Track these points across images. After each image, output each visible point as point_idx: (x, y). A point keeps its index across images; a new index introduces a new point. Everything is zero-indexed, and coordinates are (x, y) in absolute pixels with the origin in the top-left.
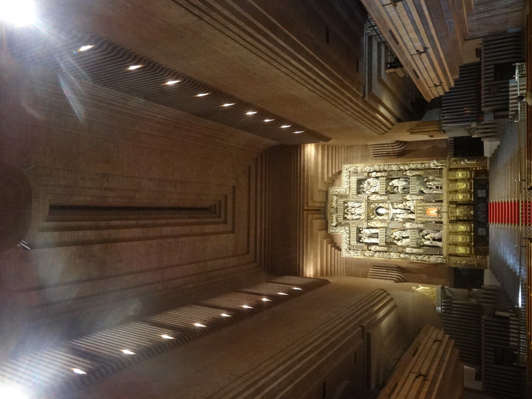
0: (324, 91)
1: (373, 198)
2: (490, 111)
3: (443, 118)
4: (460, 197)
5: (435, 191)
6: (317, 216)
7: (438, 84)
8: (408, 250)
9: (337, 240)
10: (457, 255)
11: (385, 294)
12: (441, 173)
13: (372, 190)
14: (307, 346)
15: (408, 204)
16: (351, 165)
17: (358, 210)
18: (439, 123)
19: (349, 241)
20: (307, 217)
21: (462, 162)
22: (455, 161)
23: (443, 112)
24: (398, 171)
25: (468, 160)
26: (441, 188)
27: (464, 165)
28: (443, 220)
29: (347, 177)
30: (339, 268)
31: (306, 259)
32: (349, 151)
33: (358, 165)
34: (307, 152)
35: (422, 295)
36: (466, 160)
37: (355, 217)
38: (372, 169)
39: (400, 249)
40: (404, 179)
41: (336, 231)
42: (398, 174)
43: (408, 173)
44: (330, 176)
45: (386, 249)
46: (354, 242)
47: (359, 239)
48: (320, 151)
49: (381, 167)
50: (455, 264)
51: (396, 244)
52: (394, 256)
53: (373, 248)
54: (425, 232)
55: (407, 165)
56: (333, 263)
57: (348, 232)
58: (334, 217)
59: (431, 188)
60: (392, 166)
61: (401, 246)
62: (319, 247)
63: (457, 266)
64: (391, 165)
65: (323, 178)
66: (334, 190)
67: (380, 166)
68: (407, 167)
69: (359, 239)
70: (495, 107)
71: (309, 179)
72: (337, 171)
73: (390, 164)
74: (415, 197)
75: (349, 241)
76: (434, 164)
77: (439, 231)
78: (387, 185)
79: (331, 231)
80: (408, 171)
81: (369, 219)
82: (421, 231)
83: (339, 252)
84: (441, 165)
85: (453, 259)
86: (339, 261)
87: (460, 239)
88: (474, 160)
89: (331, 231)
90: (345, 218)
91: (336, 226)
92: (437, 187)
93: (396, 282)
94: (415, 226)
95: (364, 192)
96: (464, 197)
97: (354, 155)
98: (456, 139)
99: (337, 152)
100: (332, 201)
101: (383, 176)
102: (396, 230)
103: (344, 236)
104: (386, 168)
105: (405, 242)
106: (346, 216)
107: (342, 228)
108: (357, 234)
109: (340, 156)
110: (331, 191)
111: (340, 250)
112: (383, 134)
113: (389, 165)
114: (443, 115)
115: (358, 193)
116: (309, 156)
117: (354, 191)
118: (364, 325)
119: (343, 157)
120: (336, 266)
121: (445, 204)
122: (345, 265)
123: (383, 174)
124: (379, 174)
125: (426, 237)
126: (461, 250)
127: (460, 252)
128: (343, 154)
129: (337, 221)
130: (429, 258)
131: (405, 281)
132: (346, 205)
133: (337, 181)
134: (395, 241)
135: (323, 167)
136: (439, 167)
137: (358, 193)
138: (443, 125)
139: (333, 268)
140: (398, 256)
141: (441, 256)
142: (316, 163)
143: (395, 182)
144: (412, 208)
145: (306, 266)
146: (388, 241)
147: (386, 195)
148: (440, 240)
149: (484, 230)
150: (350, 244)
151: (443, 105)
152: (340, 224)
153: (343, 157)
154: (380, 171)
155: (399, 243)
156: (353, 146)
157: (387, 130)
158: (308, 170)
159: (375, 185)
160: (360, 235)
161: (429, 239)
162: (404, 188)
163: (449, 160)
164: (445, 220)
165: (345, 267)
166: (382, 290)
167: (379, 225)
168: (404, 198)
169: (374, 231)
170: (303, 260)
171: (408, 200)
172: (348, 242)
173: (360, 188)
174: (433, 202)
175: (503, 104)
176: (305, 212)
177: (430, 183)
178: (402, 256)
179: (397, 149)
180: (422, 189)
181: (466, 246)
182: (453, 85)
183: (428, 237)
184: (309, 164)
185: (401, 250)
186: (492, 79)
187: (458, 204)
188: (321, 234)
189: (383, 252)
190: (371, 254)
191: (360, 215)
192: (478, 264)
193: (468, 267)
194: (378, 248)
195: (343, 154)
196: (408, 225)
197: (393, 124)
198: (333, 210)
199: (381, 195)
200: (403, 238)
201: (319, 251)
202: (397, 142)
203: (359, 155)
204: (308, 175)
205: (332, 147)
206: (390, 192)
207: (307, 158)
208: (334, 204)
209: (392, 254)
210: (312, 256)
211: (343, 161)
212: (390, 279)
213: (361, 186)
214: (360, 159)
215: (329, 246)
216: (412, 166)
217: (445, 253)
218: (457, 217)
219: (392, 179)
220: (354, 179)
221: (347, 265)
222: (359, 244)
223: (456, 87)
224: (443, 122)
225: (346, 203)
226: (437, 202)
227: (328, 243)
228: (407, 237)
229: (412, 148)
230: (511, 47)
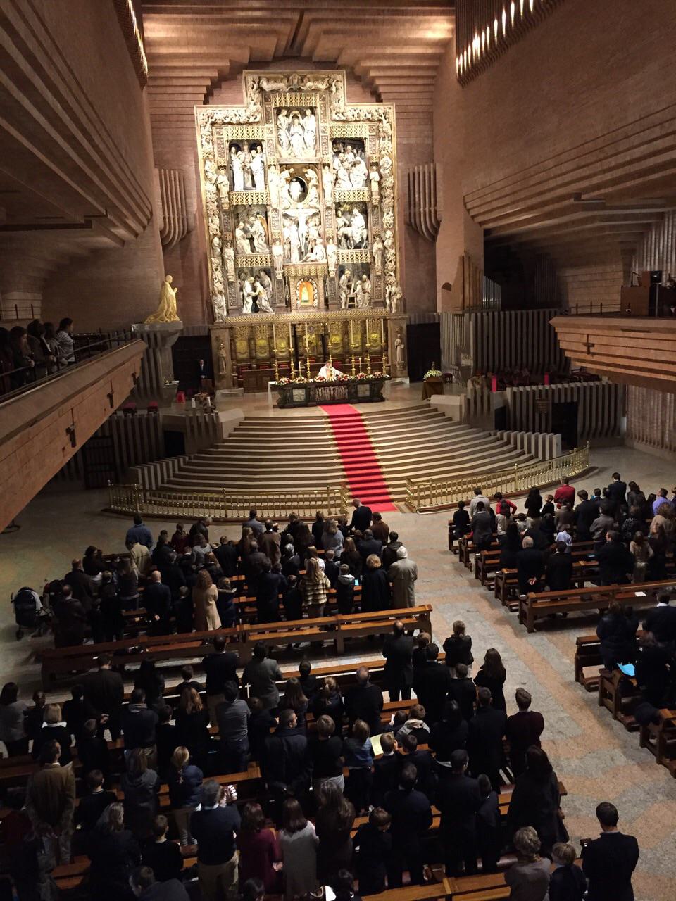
0: (635, 140)
2: (505, 401)
3: (485, 314)
4: (336, 339)
5: (344, 295)
6: (283, 43)
7: (592, 350)
8: (229, 252)
9: (225, 92)
10: (232, 340)
11: (145, 222)
12: (376, 304)
13: (342, 173)
14: (90, 140)
15: (319, 249)
16: (394, 124)
18: (477, 307)
19: (230, 123)
20: (285, 21)
21: (398, 340)
22: (401, 328)
23: (496, 314)
24: (382, 226)
25: (403, 350)
26: (350, 306)
27: (393, 343)
28: (294, 312)
29: (369, 116)
30: (165, 97)
31: (185, 21)
32: (421, 115)
33: (394, 139)
34: (435, 21)
35: (161, 296)
36: (402, 346)
37: (283, 132)
38: (388, 171)
39: (229, 234)
40: (365, 236)
41: (251, 92)
42: (375, 225)
43: (377, 246)
44: (372, 74)
45: (226, 207)
46: (228, 134)
47: (236, 145)
48: (430, 51)
49: (389, 192)
50: (218, 339)
51: (237, 225)
52: (214, 224)
53: (223, 179)
54: (267, 280)
55: (394, 243)
56: (175, 82)
57: (251, 120)
58: (281, 85)
59: (349, 287)
60: (391, 214)
61: (234, 237)
62: (213, 50)
63: (214, 344)
64: (393, 211)
65: (370, 57)
66: (340, 85)
67: (392, 188)
68: (388, 243)
69: (236, 145)
70: (511, 408)
71: (372, 27)
72: (381, 89)
73: (396, 210)
74: (332, 261)
75: (230, 123)
76: (395, 294)
77: (272, 305)
78: (351, 203)
79: (250, 79)
80: (380, 246)
82: (269, 272)
83: (202, 97)
84: (393, 305)
85: (226, 335)
86: (180, 97)
87: (261, 342)
88: (403, 359)
89: (250, 77)
90: (279, 111)
91: (261, 90)
92: (352, 300)
93: (162, 232)
94: (278, 264)
95: (337, 153)
96: (337, 344)
97: (413, 128)
98: (437, 326)
99: (421, 88)
100: (316, 79)
101: (371, 195)
102: (265, 226)
103: (241, 111)
104: (387, 201)
105: (245, 244)
106: (284, 112)
107: (258, 106)
108: (248, 140)
109: (414, 96)
110: (339, 77)
111: (206, 102)
112: (465, 204)
113: (393, 207)
114: (490, 314)
115: (335, 141)
116: (426, 26)
118: (109, 216)
119: (409, 102)
120: (169, 90)
121: (322, 314)
122: (174, 111)
123: (376, 197)
124: (375, 187)
125: (258, 284)
126: (242, 346)
127: (238, 344)
128: (418, 102)
129: (272, 91)
130: (220, 293)
131: (164, 248)
132: (308, 112)
133: (357, 89)
134: (241, 224)
135: (393, 57)
136: (388, 301)
137: (335, 141)
138: (473, 315)
139: (163, 83)
140: (215, 232)
141: (225, 313)
142: (407, 42)
143: (358, 220)
144: (312, 256)
145: (168, 20)
146: (240, 210)
148: (256, 309)
149: (303, 398)
151: (507, 313)
152: (267, 100)
153: (409, 102)
154: (381, 188)
155: (239, 233)
156: (432, 124)
157: (472, 213)
158: (394, 21)
159: (353, 180)
160: (246, 148)
161: (254, 290)
162: (347, 237)
163: (403, 319)
164: (295, 315)
165: (170, 111)
166: (151, 213)
168: (331, 241)
169: (259, 179)
170: (182, 12)
171: (325, 248)
172: (228, 120)
173: (345, 146)
174: (325, 293)
175: (515, 422)
176: (296, 16)
177: (359, 287)
178: (216, 241)
179: (424, 224)
180: (348, 272)
181: (250, 353)
182: (567, 354)
183: (260, 288)
184: (408, 25)
185: (227, 239)
186: (556, 401)
187: (323, 338)
188: (244, 56)
189: (218, 200)
190: (209, 175)
192: (223, 377)
193: (215, 359)
194: (225, 190)
195: (418, 102)
197: (481, 224)
198: (296, 81)
200: (251, 239)
201: (204, 50)
202: (438, 223)
203: (413, 141)
204: (383, 22)
205: (433, 77)
207: (421, 22)
208: (309, 84)
209: (217, 220)
210: (192, 35)
211: (401, 103)
212: (164, 218)
213: (349, 147)
214: (405, 142)
215: (215, 74)
216: (390, 253)
217: (234, 319)
218: (301, 337)
219: (364, 212)
220: (364, 131)
221: (175, 118)
222: (226, 145)
223: (564, 360)
224: (479, 314)
225: (313, 113)
226: (326, 301)
227: (220, 70)
228: (253, 249)
230: (600, 423)
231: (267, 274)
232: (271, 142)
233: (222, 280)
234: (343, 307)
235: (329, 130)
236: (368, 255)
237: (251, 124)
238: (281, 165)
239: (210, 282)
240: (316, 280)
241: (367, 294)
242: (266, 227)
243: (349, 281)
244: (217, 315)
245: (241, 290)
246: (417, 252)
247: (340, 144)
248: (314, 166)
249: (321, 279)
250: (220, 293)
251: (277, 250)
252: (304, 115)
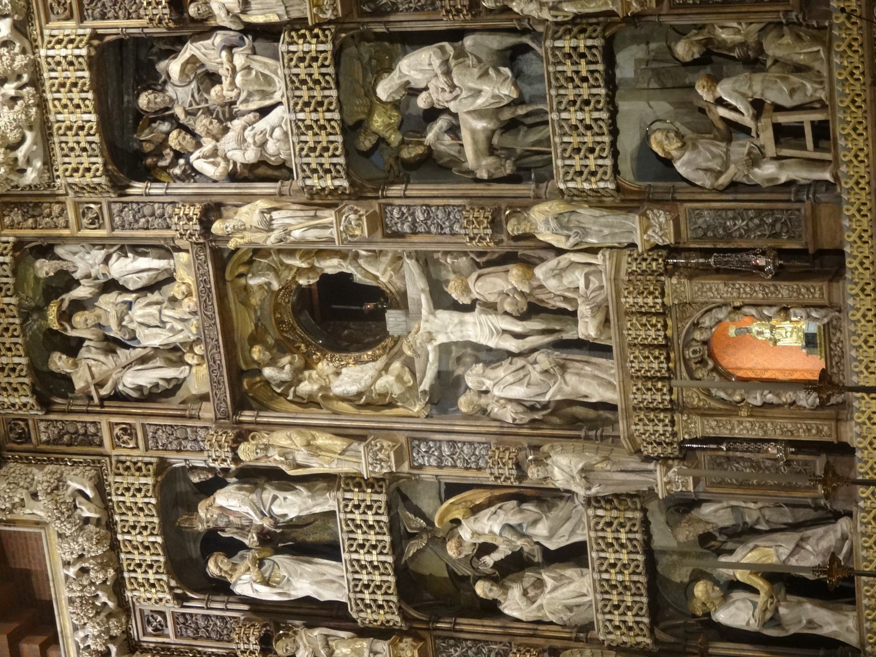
1: (247, 221)
15: (552, 280)
17: (149, 320)
19: (118, 588)
40: (496, 42)
51: (491, 609)
74: (600, 226)
81: (245, 394)
90: (51, 388)
106: (59, 362)
117: (82, 162)
132: (44, 268)
134: (482, 589)
147: (357, 194)
150: (125, 608)
152: (25, 437)
167: (331, 456)
169: (292, 505)
174: (753, 273)
191: (174, 354)
196: (563, 467)
199: (317, 201)
206: (382, 161)
213: (144, 100)
222: (197, 607)
225: (46, 250)
232: (162, 438)
234: (827, 176)
235: (86, 197)
236: (566, 44)
237: (107, 507)
238: (240, 402)
241: (774, 49)
242: (480, 497)
247: (130, 155)
248: (224, 265)
251: (563, 467)
252: (66, 281)
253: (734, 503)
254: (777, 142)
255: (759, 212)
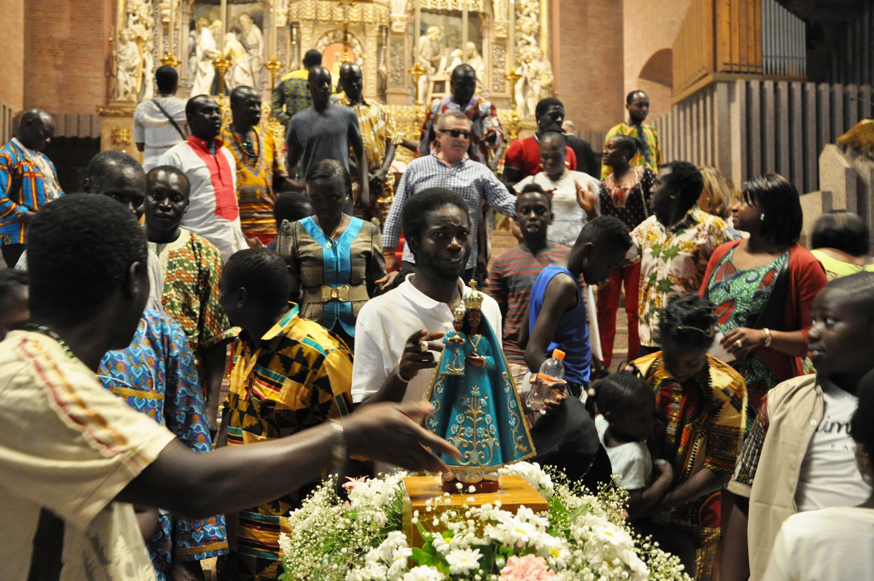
54: (254, 34)
130: (138, 39)
136: (519, 98)
224: (755, 85)
229: (592, 9)
231: (255, 23)
233: (151, 21)
239: (120, 19)
240: (360, 37)
243: (436, 54)
244: (122, 87)
245: (193, 51)
246: (583, 13)
249: (373, 33)
250: (138, 39)
253: (261, 45)
254: (436, 83)
255: (402, 70)
